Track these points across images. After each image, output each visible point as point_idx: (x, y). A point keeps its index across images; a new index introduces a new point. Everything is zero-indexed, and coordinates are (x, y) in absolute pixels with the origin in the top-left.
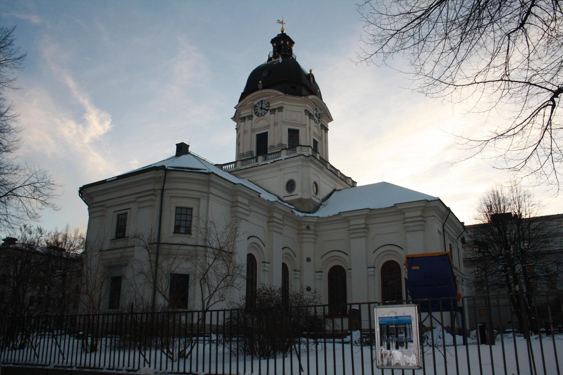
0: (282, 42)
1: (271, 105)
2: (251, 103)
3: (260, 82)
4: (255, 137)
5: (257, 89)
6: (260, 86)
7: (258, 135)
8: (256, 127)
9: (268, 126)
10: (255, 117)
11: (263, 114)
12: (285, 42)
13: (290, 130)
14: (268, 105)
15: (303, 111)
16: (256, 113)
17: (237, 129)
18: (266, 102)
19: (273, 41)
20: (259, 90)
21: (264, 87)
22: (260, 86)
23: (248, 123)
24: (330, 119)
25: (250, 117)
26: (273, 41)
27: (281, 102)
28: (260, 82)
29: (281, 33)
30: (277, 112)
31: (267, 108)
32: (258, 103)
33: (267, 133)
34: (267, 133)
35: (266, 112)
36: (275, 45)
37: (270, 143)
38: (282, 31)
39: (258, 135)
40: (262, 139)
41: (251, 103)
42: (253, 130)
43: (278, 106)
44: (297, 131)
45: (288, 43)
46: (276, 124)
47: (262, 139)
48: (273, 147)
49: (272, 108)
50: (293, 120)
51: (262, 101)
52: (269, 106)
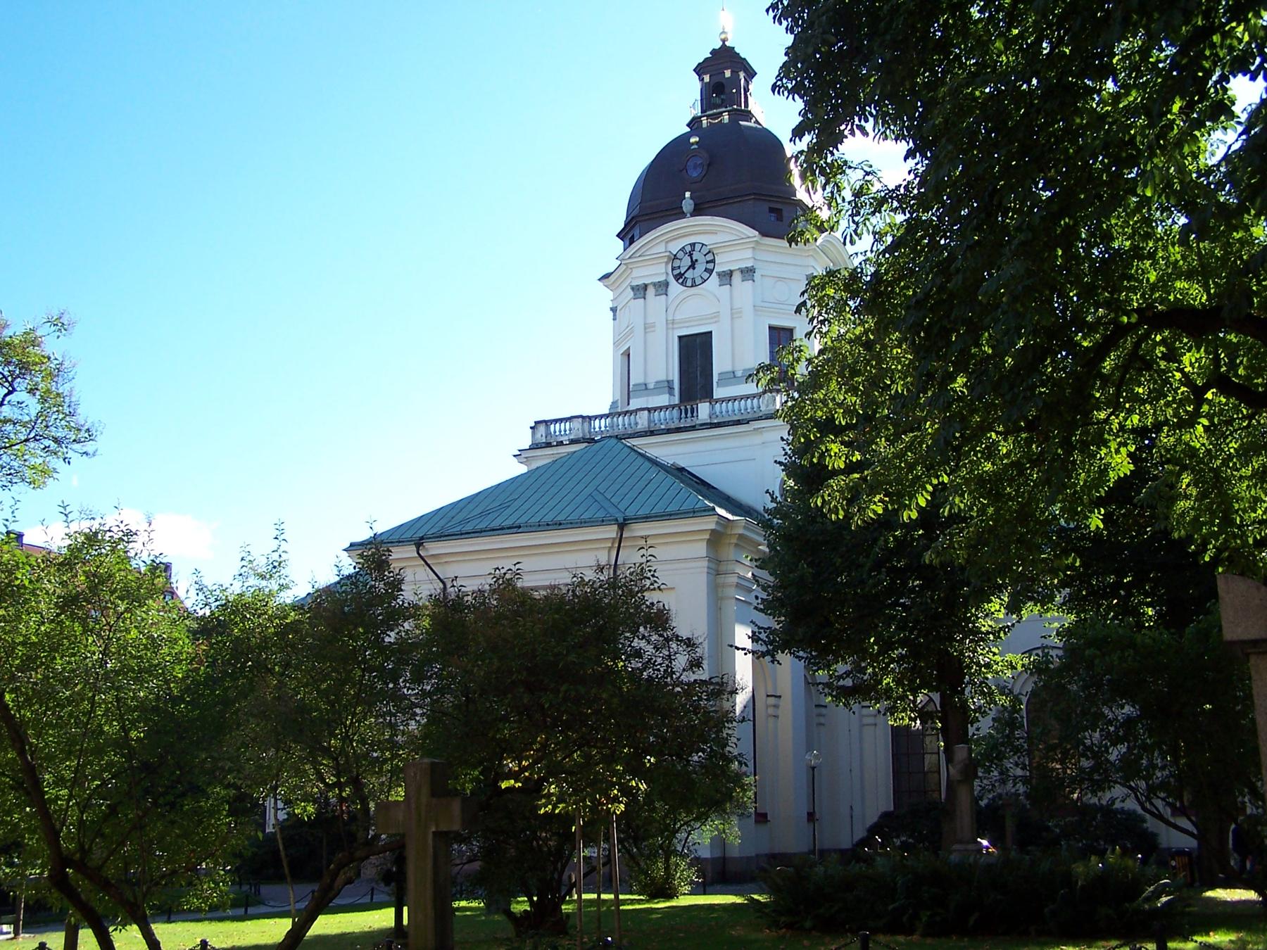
0: (728, 74)
2: (661, 248)
3: (688, 194)
4: (676, 340)
6: (688, 205)
7: (680, 337)
8: (678, 317)
9: (715, 317)
10: (675, 287)
11: (698, 281)
13: (771, 328)
14: (709, 257)
16: (678, 277)
17: (614, 310)
18: (705, 250)
19: (700, 70)
21: (698, 211)
22: (688, 205)
23: (654, 301)
25: (662, 287)
26: (700, 70)
28: (688, 194)
29: (718, 45)
31: (710, 266)
32: (682, 249)
35: (706, 275)
36: (707, 78)
37: (721, 362)
38: (724, 41)
39: (680, 337)
40: (696, 351)
41: (661, 248)
42: (671, 324)
43: (743, 266)
46: (735, 314)
47: (696, 351)
48: (730, 377)
49: (726, 268)
51: (693, 245)
52: (713, 261)
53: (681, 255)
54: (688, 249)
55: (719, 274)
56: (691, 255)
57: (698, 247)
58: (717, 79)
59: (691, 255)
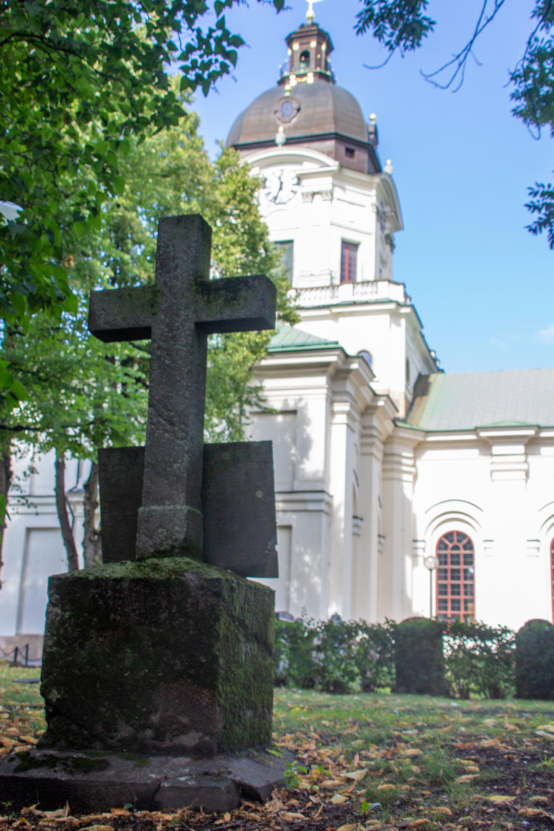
1: (304, 182)
6: (280, 138)
12: (319, 44)
21: (289, 142)
24: (398, 227)
33: (291, 242)
55: (303, 194)
56: (280, 178)
58: (305, 48)
59: (280, 178)
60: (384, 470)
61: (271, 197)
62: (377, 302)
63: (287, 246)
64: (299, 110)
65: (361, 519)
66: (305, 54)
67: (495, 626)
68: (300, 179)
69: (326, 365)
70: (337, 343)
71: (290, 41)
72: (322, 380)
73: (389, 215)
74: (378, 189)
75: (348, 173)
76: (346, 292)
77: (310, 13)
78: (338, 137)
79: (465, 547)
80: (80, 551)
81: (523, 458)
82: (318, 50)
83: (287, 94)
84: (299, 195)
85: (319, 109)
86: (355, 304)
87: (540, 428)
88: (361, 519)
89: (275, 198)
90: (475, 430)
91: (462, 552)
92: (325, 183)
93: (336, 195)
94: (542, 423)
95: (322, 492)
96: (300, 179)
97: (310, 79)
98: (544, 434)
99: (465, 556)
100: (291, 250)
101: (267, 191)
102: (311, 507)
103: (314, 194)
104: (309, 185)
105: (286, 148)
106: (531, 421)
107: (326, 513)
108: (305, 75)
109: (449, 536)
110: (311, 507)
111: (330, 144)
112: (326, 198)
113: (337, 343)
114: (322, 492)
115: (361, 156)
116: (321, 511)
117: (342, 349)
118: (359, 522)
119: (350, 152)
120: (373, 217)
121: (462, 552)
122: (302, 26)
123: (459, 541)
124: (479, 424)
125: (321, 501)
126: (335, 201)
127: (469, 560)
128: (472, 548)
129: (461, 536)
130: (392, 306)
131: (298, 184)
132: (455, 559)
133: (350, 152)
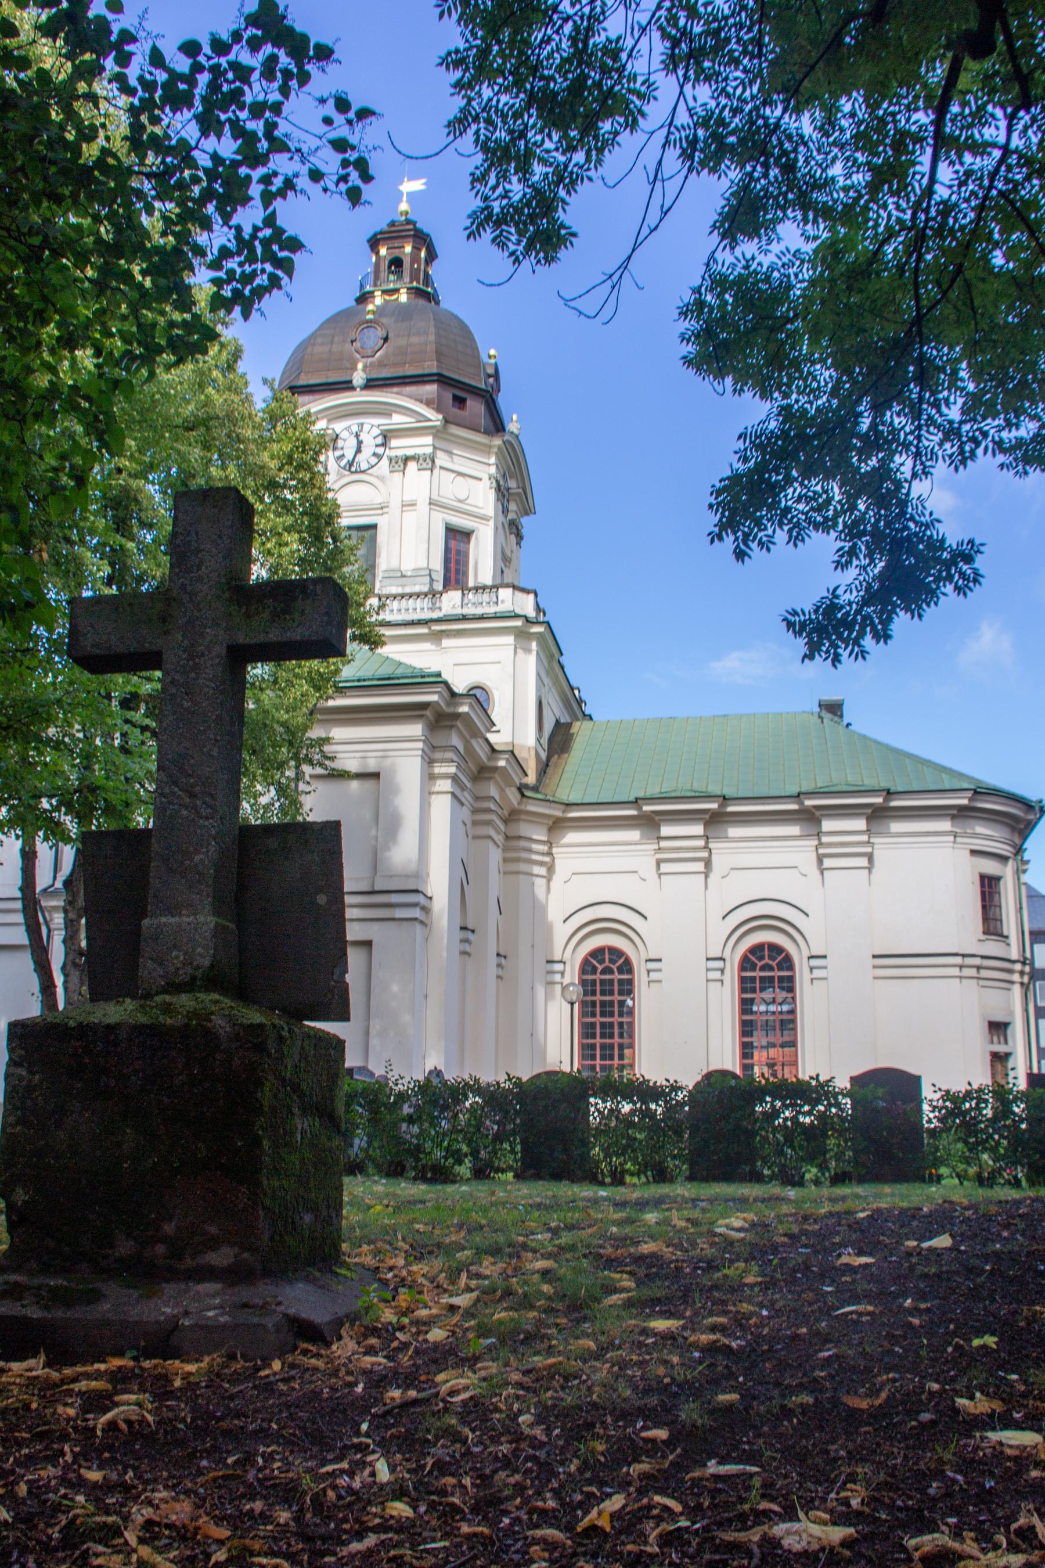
0: (408, 249)
1: (394, 443)
5: (346, 386)
6: (359, 378)
9: (382, 507)
12: (416, 249)
15: (485, 477)
20: (353, 389)
21: (370, 385)
24: (527, 510)
27: (429, 440)
30: (412, 466)
32: (348, 428)
33: (374, 527)
34: (374, 527)
44: (466, 535)
45: (423, 254)
49: (400, 453)
50: (460, 501)
53: (344, 435)
54: (355, 429)
55: (391, 460)
56: (357, 436)
57: (366, 428)
58: (396, 253)
59: (357, 436)
60: (505, 860)
61: (343, 463)
62: (496, 617)
63: (367, 534)
64: (386, 340)
65: (473, 931)
66: (397, 263)
67: (661, 1081)
68: (386, 437)
69: (424, 706)
70: (439, 675)
71: (374, 243)
72: (416, 729)
73: (515, 493)
74: (499, 455)
75: (454, 430)
76: (451, 602)
77: (404, 206)
78: (442, 379)
79: (620, 971)
80: (59, 979)
81: (701, 843)
82: (415, 257)
83: (370, 317)
84: (385, 462)
85: (414, 340)
86: (464, 618)
87: (725, 799)
88: (473, 931)
89: (351, 464)
90: (636, 802)
91: (617, 976)
92: (423, 444)
93: (438, 462)
94: (728, 792)
95: (417, 891)
96: (386, 437)
97: (403, 297)
98: (731, 809)
99: (621, 982)
100: (374, 539)
101: (338, 453)
102: (399, 913)
103: (407, 459)
104: (401, 446)
105: (364, 392)
106: (714, 789)
107: (422, 922)
108: (396, 291)
109: (597, 953)
110: (399, 913)
111: (432, 389)
112: (425, 465)
113: (439, 675)
114: (417, 891)
115: (475, 407)
116: (416, 919)
117: (446, 683)
118: (470, 936)
119: (459, 401)
120: (492, 495)
121: (617, 976)
122: (393, 224)
123: (611, 961)
124: (641, 795)
125: (415, 905)
126: (436, 471)
127: (627, 988)
128: (630, 971)
129: (616, 953)
130: (518, 623)
131: (384, 445)
132: (607, 986)
133: (459, 401)
